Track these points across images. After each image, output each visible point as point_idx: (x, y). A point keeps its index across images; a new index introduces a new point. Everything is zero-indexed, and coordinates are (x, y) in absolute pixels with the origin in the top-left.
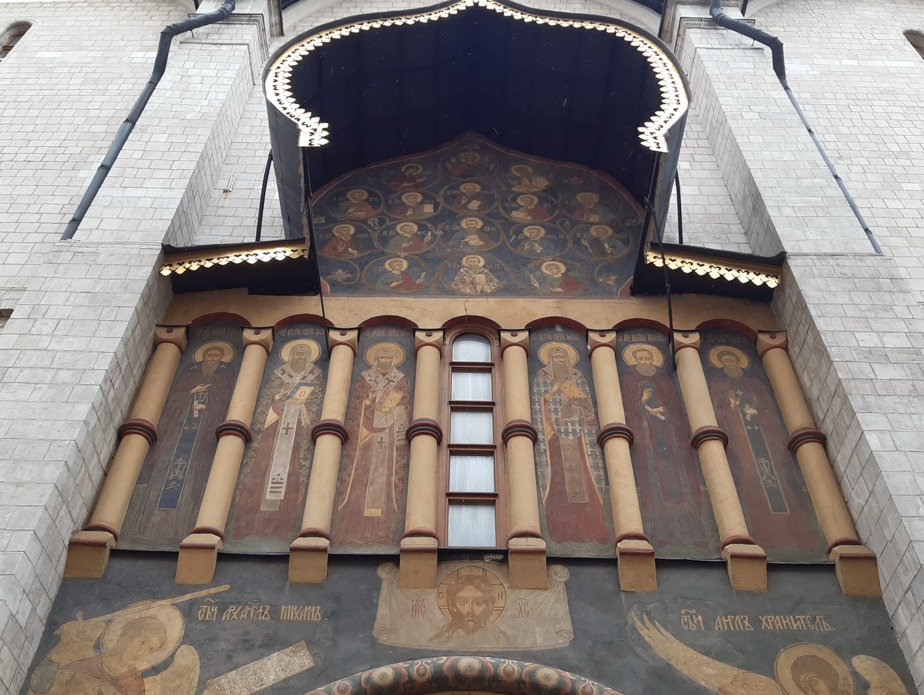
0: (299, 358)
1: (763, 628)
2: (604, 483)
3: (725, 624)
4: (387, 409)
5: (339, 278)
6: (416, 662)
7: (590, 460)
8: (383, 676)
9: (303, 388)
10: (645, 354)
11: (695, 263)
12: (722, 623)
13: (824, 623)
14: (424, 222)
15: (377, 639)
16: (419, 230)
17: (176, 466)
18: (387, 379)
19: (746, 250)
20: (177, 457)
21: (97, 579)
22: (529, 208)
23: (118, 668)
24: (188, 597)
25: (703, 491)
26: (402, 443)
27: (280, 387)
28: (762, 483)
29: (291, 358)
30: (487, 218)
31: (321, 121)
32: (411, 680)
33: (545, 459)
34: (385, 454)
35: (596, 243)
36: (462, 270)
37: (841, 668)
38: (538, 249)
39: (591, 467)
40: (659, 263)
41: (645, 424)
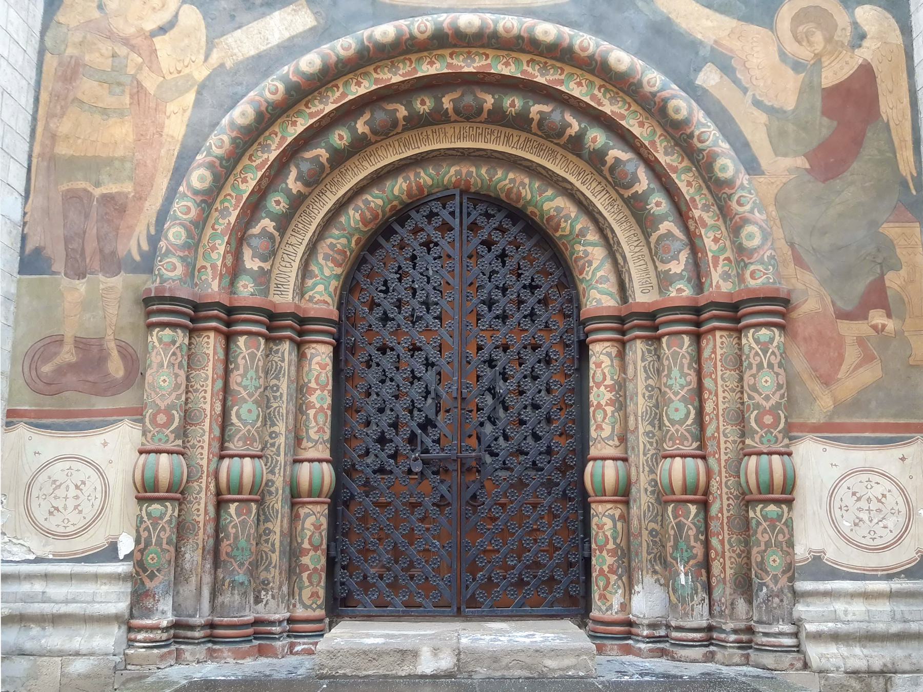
6: (416, 19)
32: (412, 38)
37: (841, 18)
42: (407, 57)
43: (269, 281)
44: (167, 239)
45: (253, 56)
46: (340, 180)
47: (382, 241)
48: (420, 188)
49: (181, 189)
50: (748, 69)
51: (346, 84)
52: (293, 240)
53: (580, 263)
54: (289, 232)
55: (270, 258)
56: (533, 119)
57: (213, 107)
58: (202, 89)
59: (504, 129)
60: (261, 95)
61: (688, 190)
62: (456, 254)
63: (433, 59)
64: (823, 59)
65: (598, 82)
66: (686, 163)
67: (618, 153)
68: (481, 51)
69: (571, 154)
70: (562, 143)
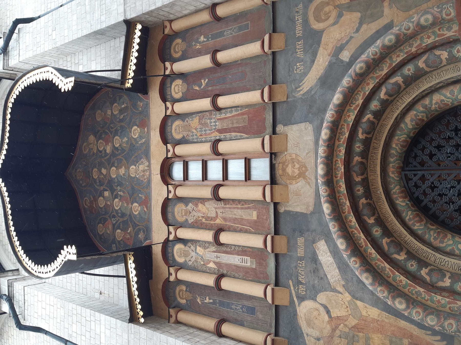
0: (183, 253)
1: (302, 35)
2: (238, 108)
3: (300, 53)
4: (207, 210)
5: (143, 236)
6: (321, 194)
7: (228, 114)
8: (327, 208)
9: (198, 251)
10: (176, 88)
11: (130, 64)
12: (300, 54)
13: (299, 7)
15: (311, 211)
18: (192, 211)
19: (123, 39)
20: (231, 308)
21: (288, 342)
22: (105, 144)
23: (328, 328)
24: (295, 299)
25: (240, 62)
26: (222, 203)
28: (236, 34)
29: (183, 257)
30: (110, 165)
32: (329, 196)
33: (228, 136)
34: (228, 211)
35: (121, 111)
36: (137, 177)
38: (125, 139)
39: (231, 114)
40: (131, 81)
41: (210, 88)
42: (337, 198)
43: (457, 274)
44: (434, 326)
45: (339, 271)
46: (398, 233)
47: (431, 212)
48: (402, 192)
49: (406, 314)
50: (342, 38)
51: (351, 227)
52: (433, 259)
53: (442, 106)
54: (428, 261)
55: (443, 272)
56: (366, 137)
57: (364, 293)
58: (354, 297)
59: (371, 151)
60: (357, 269)
61: (401, 56)
62: (438, 173)
63: (338, 186)
64: (337, 4)
65: (348, 107)
66: (387, 60)
67: (382, 94)
68: (334, 163)
69: (383, 117)
70: (377, 122)
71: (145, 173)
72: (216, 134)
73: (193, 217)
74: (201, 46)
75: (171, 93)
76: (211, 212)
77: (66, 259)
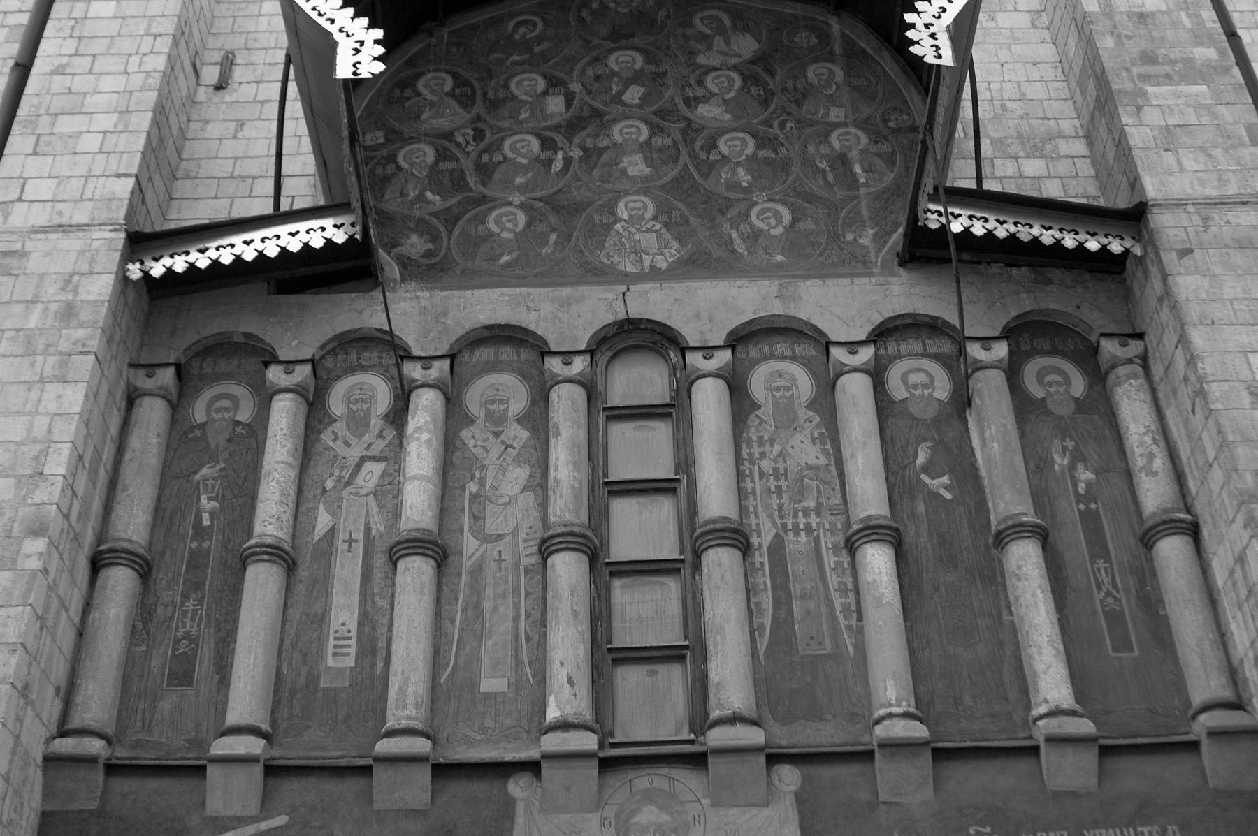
0: (358, 410)
2: (855, 616)
4: (506, 500)
5: (413, 251)
7: (834, 577)
14: (549, 133)
16: (542, 150)
17: (185, 613)
18: (503, 442)
20: (185, 597)
22: (727, 97)
27: (332, 466)
30: (656, 120)
31: (371, 25)
34: (507, 582)
36: (618, 226)
38: (744, 177)
39: (835, 590)
41: (921, 508)
71: (629, 256)
72: (769, 531)
73: (483, 447)
74: (1062, 472)
75: (904, 356)
76: (502, 518)
77: (338, 36)
